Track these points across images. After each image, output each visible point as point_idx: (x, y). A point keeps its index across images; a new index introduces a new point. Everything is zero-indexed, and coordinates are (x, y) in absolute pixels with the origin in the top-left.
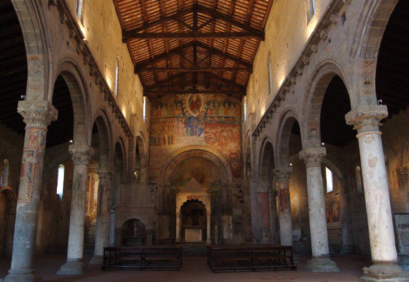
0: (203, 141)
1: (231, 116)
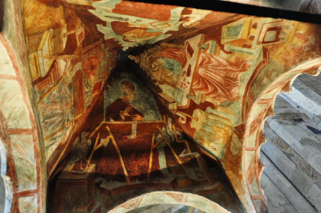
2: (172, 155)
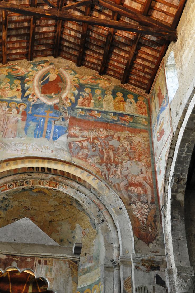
0: (61, 149)
1: (128, 113)
2: (37, 287)
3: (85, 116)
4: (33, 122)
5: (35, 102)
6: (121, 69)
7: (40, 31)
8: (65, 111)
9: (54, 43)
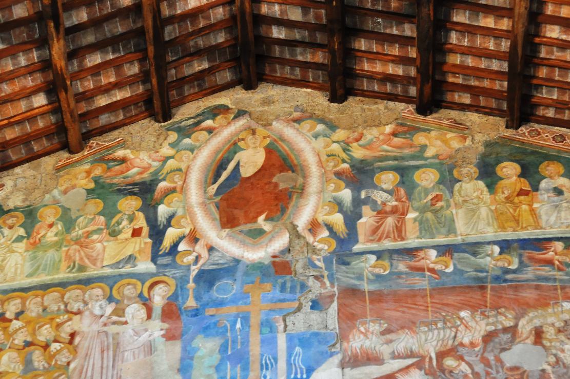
3: (394, 277)
4: (207, 336)
5: (204, 264)
6: (493, 76)
7: (179, 12)
8: (315, 274)
9: (236, 39)
